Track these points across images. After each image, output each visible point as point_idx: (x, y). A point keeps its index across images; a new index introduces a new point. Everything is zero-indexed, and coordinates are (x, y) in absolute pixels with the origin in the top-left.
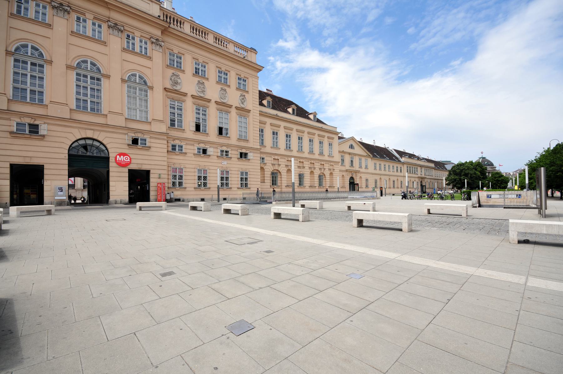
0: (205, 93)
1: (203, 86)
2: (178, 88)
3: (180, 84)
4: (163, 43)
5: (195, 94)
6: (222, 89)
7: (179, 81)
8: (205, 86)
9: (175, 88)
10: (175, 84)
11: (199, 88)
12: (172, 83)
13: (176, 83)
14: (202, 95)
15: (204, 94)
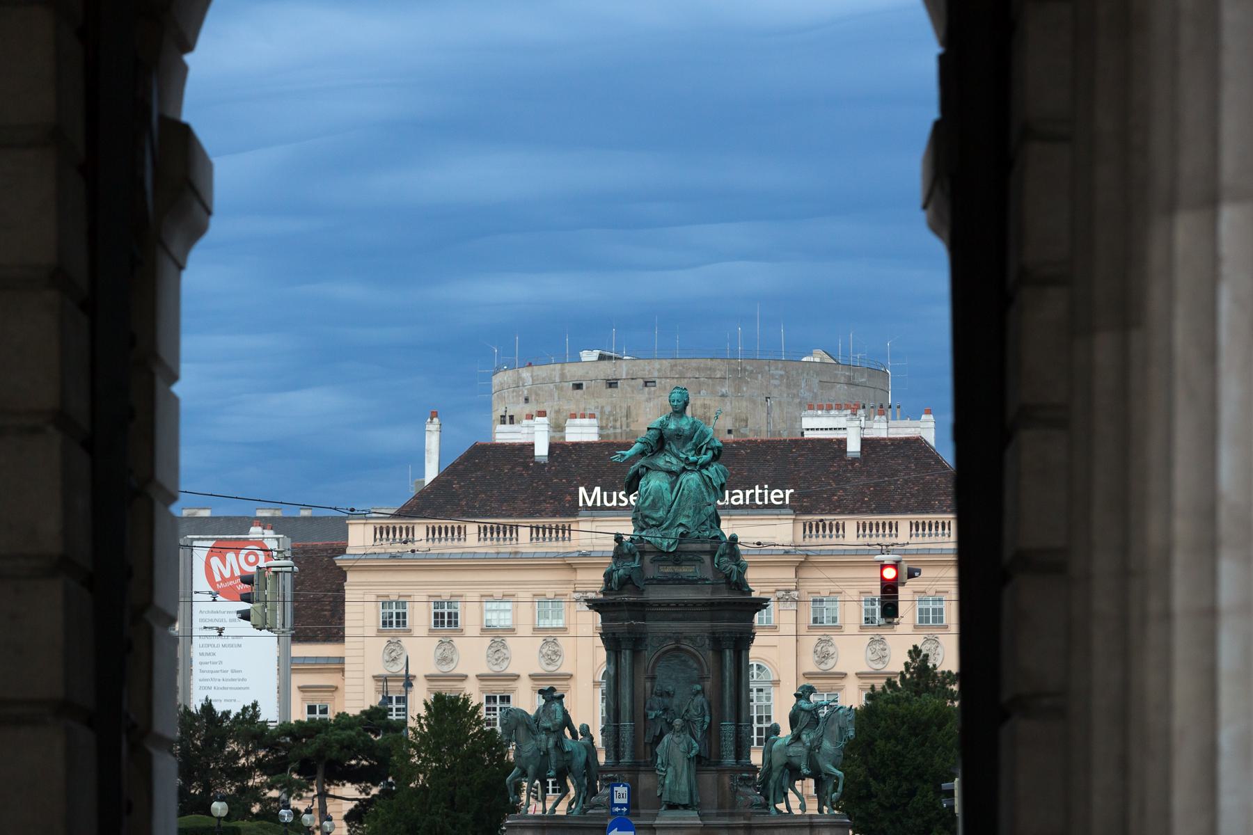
0: (887, 659)
1: (882, 646)
2: (828, 665)
3: (834, 656)
4: (796, 593)
5: (865, 668)
6: (928, 640)
7: (831, 650)
8: (885, 645)
9: (823, 667)
10: (823, 659)
11: (872, 653)
12: (817, 659)
13: (825, 656)
14: (879, 666)
15: (884, 663)
